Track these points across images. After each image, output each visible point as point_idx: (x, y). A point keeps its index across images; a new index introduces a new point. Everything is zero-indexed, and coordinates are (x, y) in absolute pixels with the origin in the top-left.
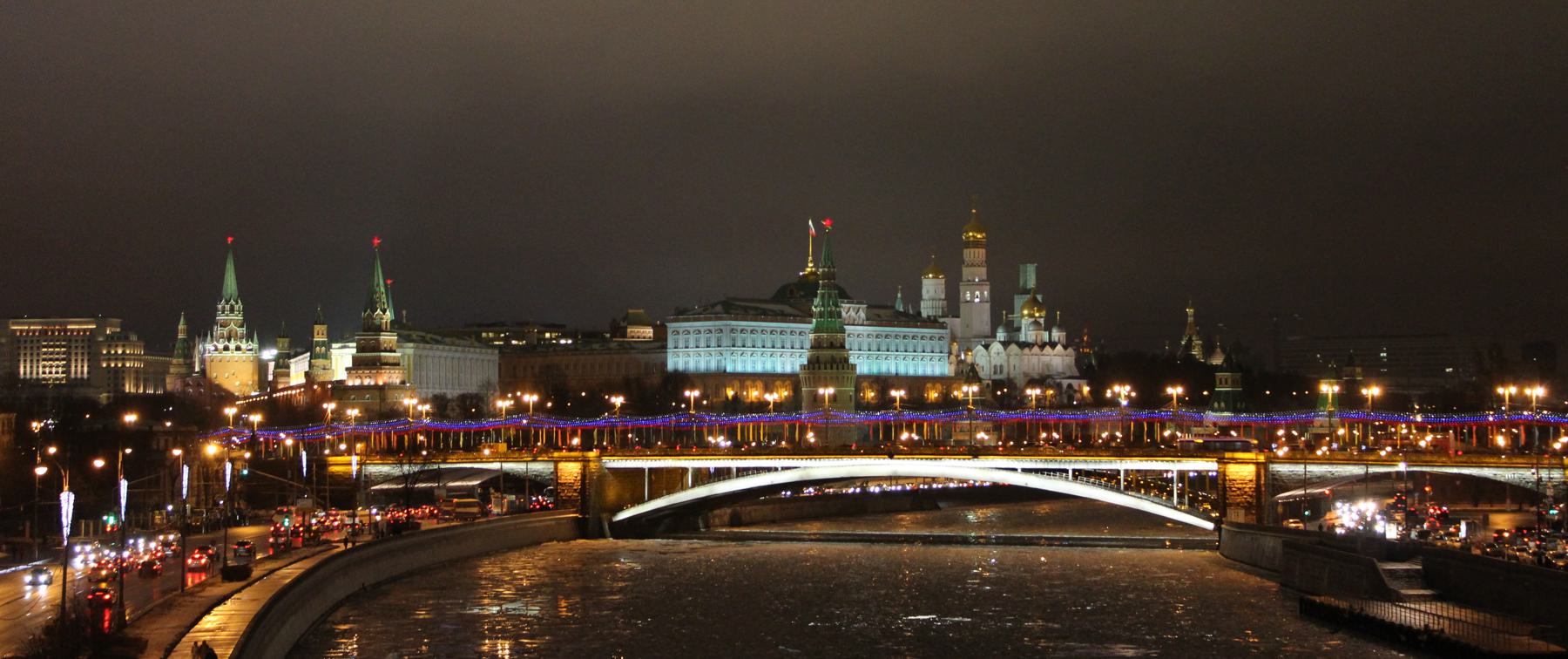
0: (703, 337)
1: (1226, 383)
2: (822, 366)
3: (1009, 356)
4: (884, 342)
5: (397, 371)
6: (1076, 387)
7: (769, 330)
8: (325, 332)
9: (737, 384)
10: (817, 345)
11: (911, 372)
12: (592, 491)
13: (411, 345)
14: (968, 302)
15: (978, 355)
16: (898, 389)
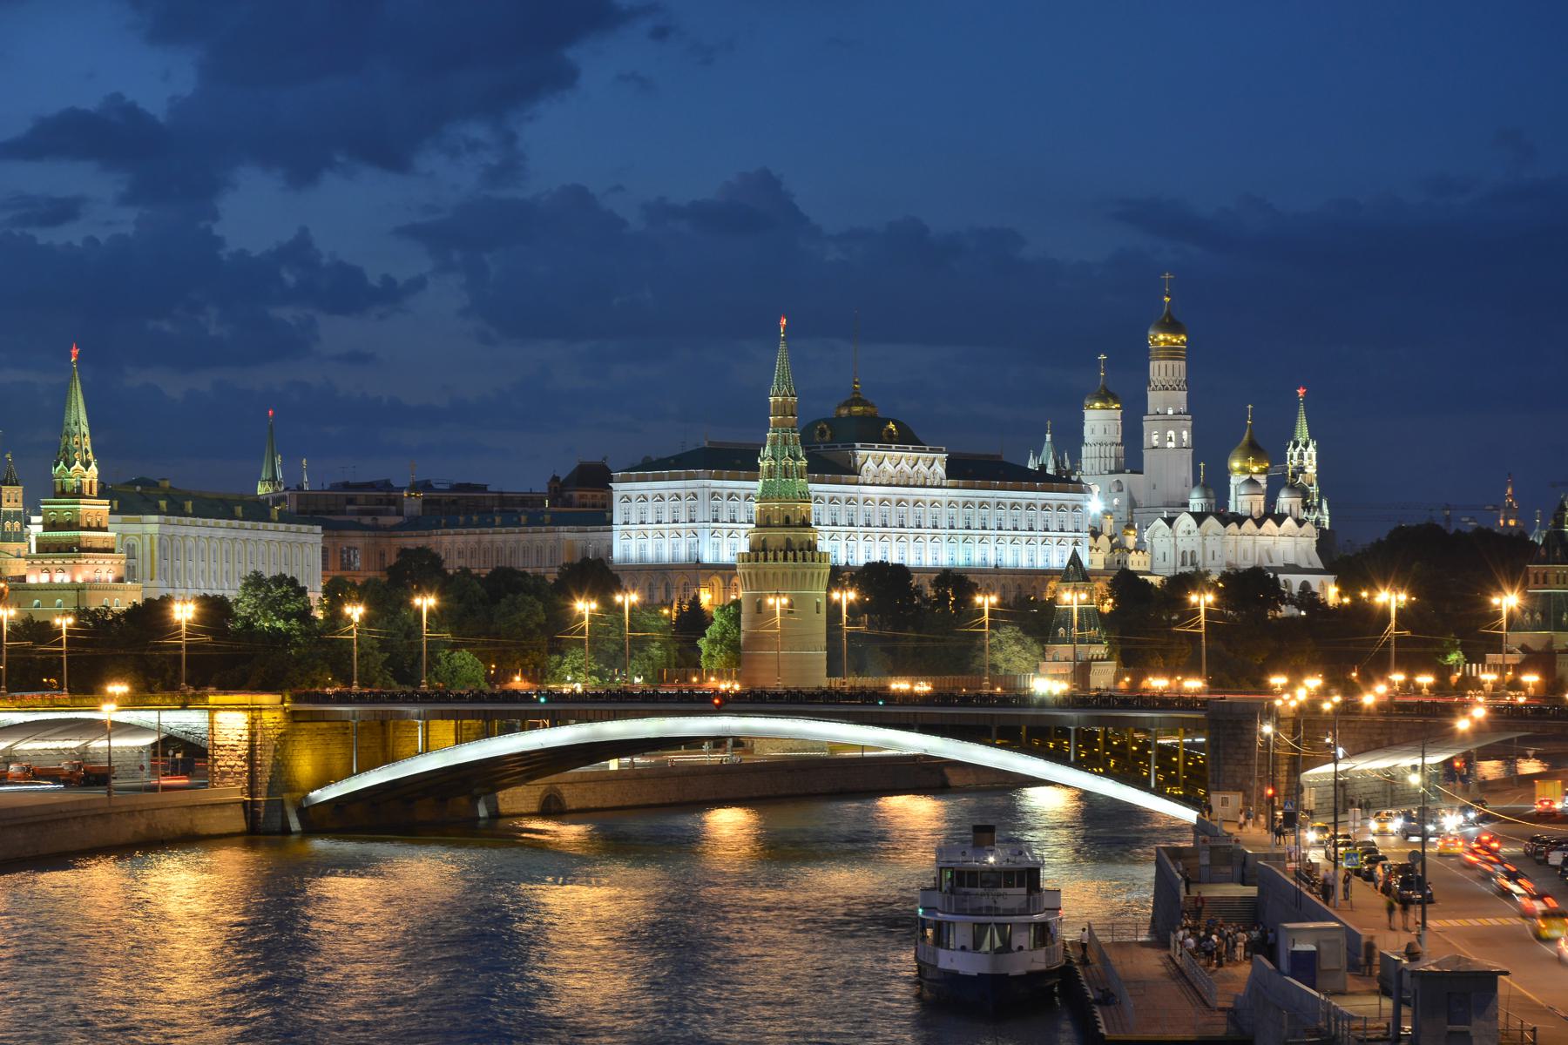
0: (667, 505)
1: (1545, 582)
2: (770, 555)
3: (1204, 536)
4: (976, 516)
5: (108, 562)
6: (1315, 588)
8: (20, 499)
9: (717, 581)
11: (1024, 563)
12: (266, 759)
13: (155, 518)
14: (1156, 448)
15: (1158, 534)
16: (987, 593)
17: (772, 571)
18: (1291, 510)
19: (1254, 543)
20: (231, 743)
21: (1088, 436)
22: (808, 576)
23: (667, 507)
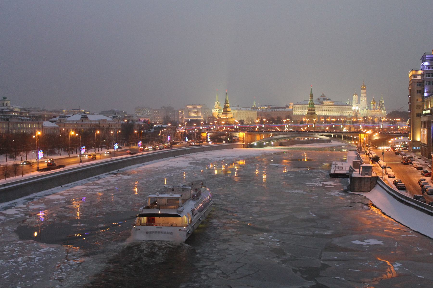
0: (299, 108)
3: (367, 112)
21: (353, 99)
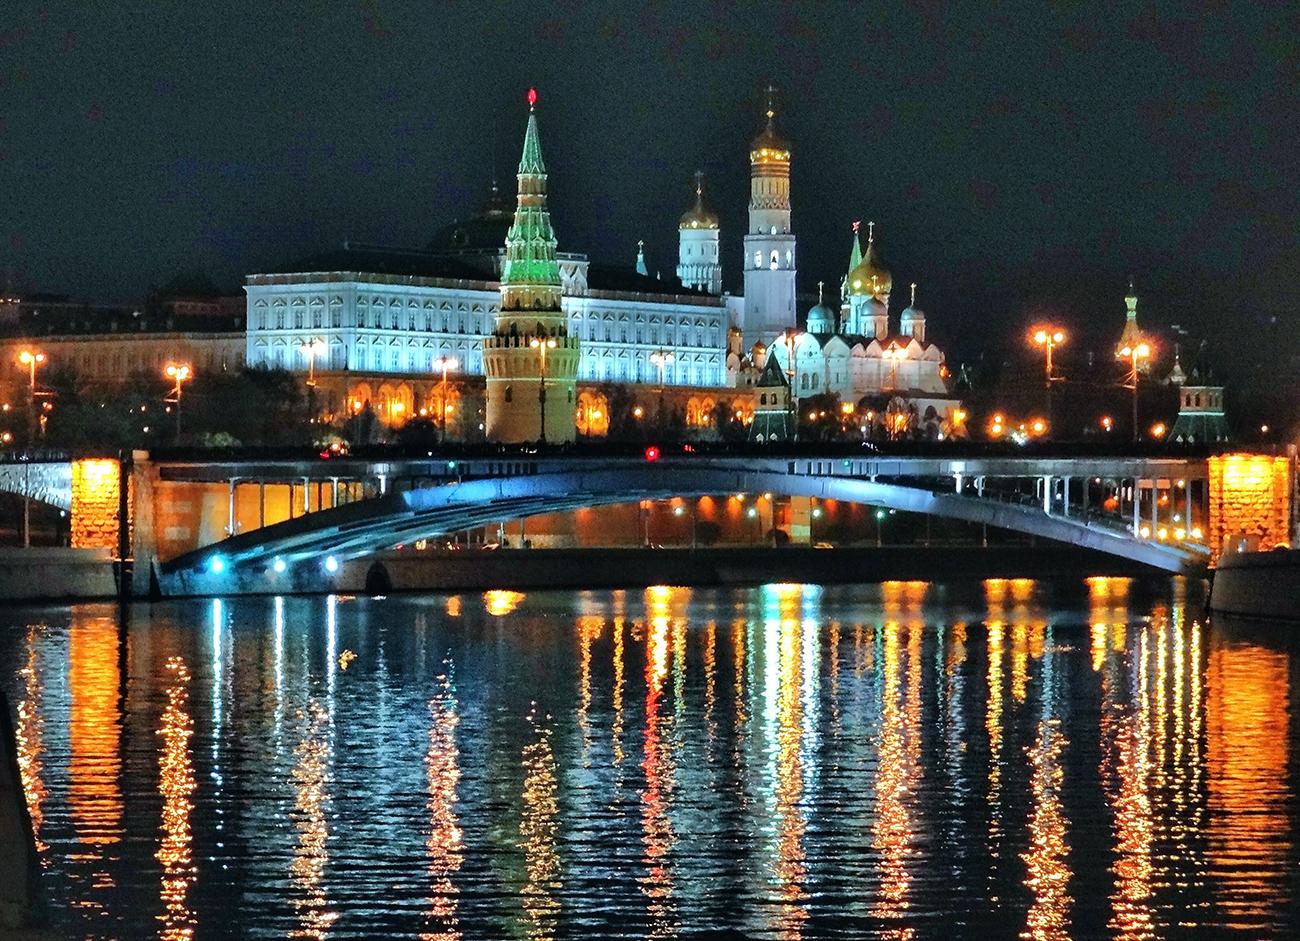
2: (522, 340)
3: (828, 357)
4: (617, 327)
7: (421, 300)
10: (513, 306)
14: (757, 269)
17: (524, 358)
18: (914, 332)
19: (879, 366)
20: (98, 500)
22: (561, 362)
23: (308, 312)
